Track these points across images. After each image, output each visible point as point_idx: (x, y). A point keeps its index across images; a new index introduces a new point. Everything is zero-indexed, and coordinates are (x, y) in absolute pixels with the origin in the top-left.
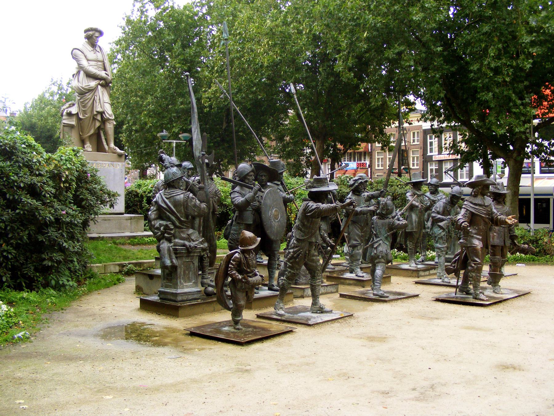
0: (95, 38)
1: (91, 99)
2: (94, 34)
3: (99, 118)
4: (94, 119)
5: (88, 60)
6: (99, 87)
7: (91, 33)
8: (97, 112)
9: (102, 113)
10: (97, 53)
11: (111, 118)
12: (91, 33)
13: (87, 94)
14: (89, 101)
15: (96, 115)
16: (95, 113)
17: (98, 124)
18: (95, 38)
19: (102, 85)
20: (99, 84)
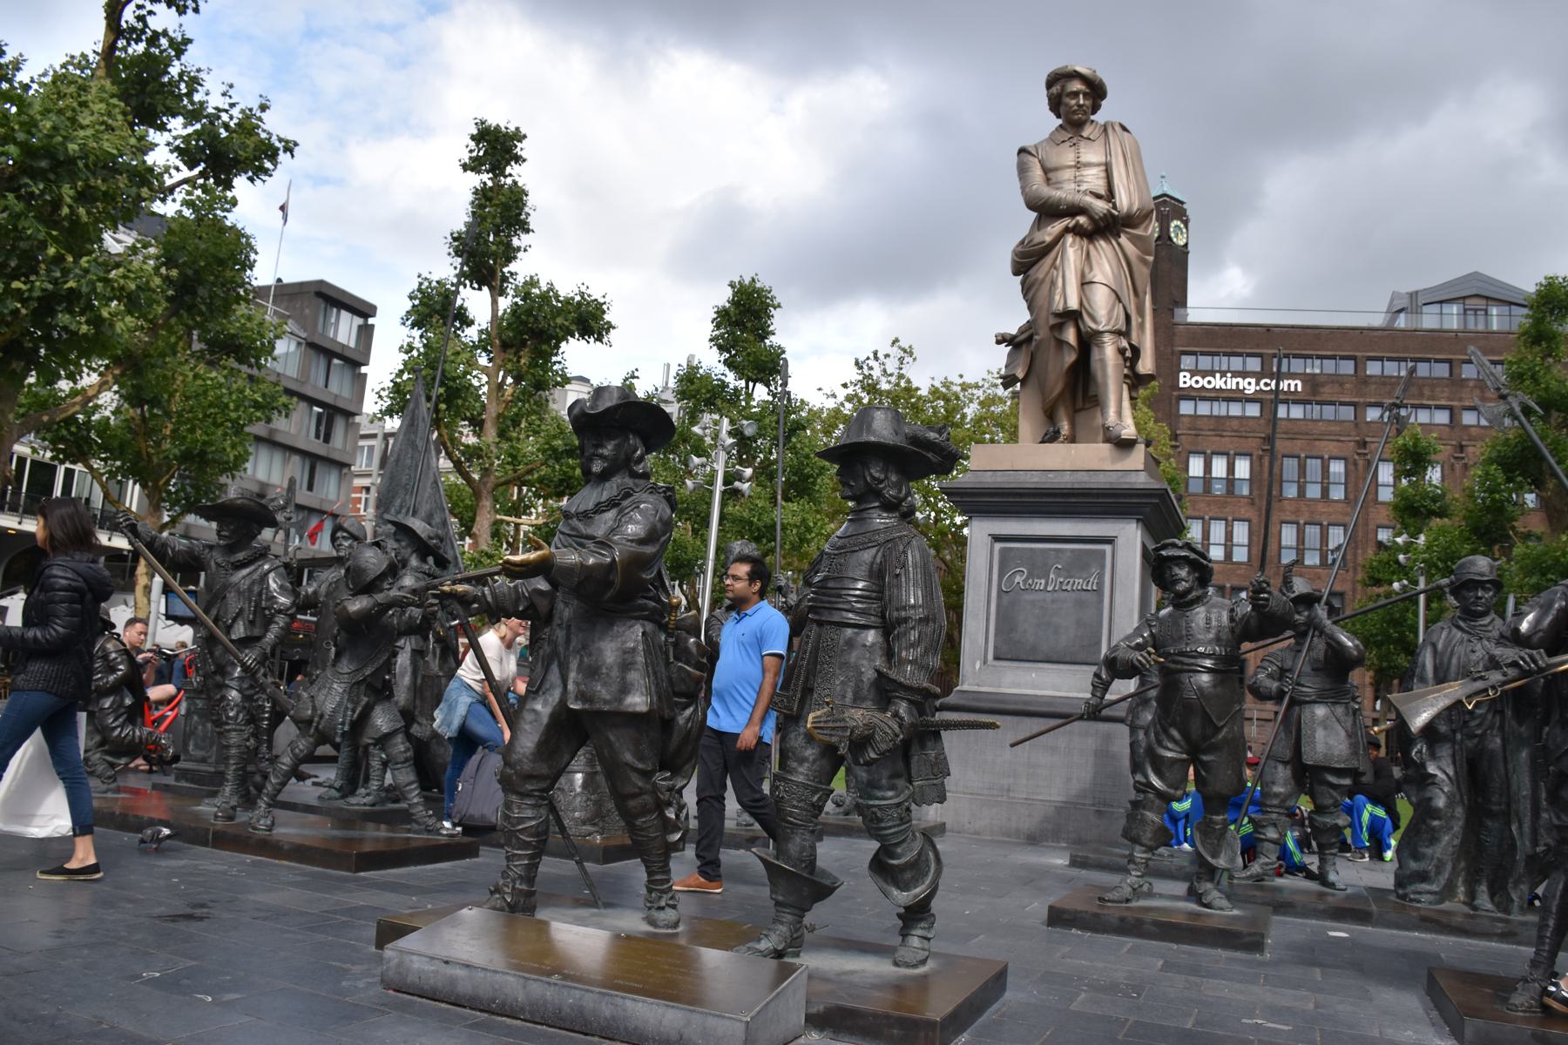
0: (1067, 100)
1: (1043, 281)
2: (1063, 88)
3: (1070, 335)
4: (1061, 343)
5: (1046, 171)
6: (1069, 239)
7: (1055, 90)
8: (1057, 315)
9: (1073, 316)
10: (1082, 143)
11: (1093, 326)
12: (1055, 90)
13: (1031, 272)
14: (1038, 290)
15: (1059, 327)
16: (1053, 321)
17: (1070, 358)
18: (1067, 100)
19: (1077, 231)
20: (1067, 230)
